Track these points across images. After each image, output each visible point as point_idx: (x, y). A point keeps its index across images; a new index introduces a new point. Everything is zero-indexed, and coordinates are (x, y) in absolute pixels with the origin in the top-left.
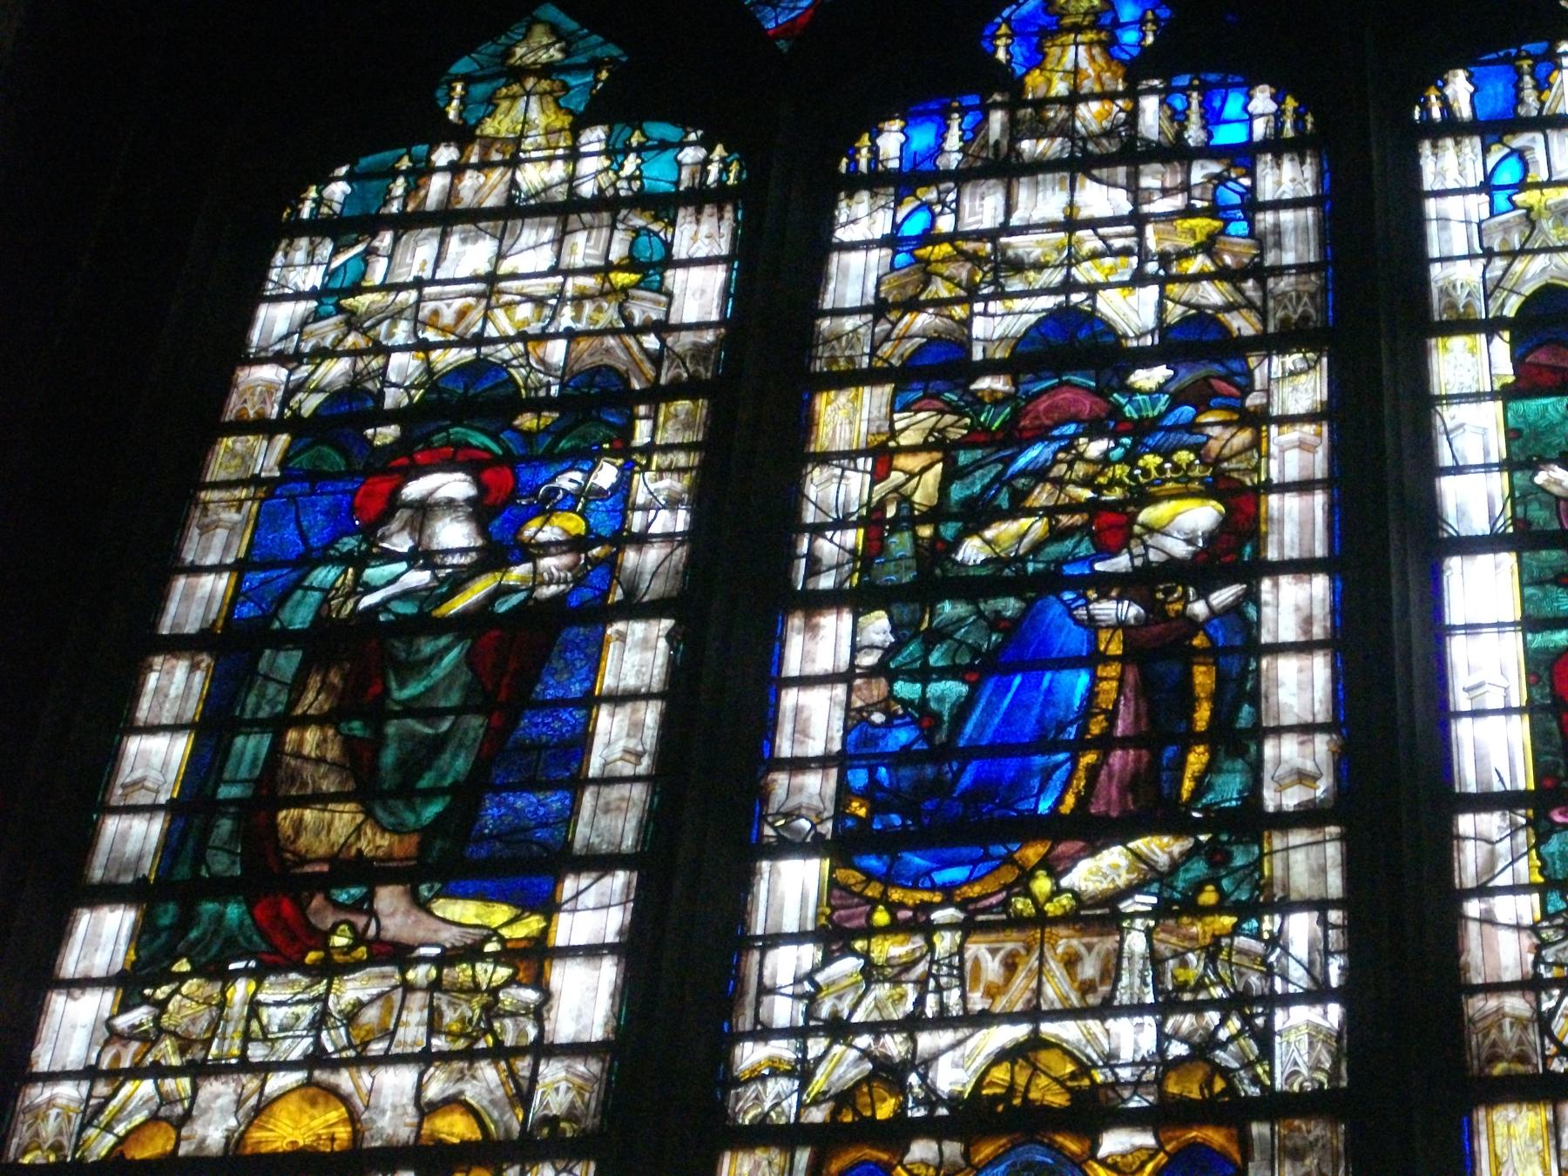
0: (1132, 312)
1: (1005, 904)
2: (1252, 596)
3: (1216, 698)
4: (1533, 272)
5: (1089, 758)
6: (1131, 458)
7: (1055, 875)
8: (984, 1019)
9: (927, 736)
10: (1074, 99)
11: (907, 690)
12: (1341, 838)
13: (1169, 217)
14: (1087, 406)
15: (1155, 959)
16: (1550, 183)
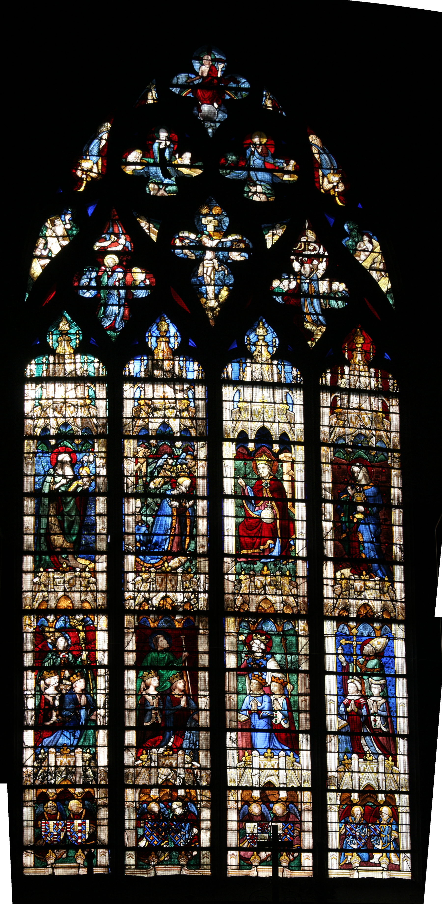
0: (175, 425)
1: (161, 568)
2: (195, 503)
3: (190, 526)
4: (240, 426)
5: (172, 538)
6: (176, 465)
7: (168, 563)
8: (159, 592)
9: (148, 529)
10: (163, 360)
11: (144, 518)
12: (208, 560)
13: (180, 399)
14: (168, 450)
15: (182, 582)
16: (243, 402)
